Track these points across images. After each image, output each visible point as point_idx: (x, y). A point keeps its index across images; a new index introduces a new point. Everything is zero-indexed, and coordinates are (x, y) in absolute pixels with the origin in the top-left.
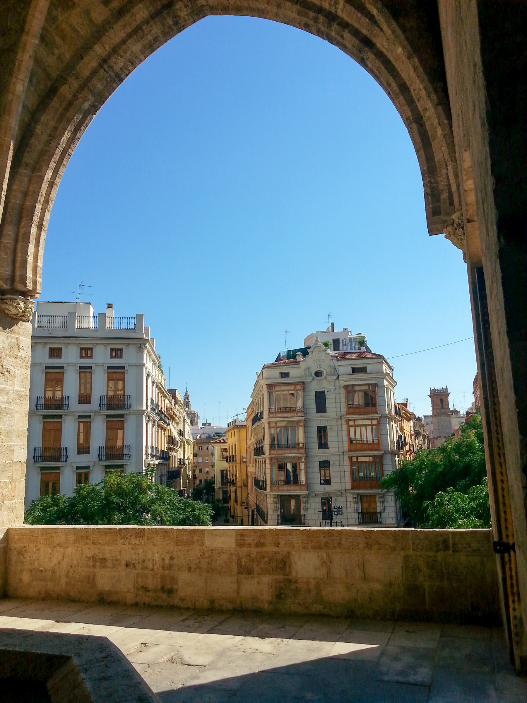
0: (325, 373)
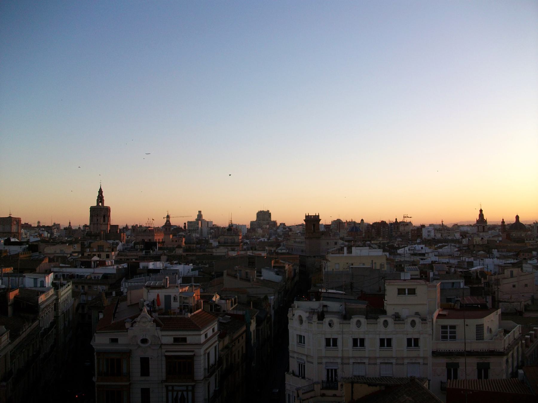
0: (150, 342)
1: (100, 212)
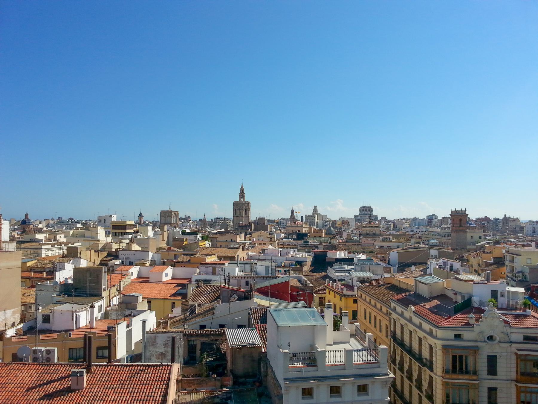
0: (498, 339)
1: (241, 207)
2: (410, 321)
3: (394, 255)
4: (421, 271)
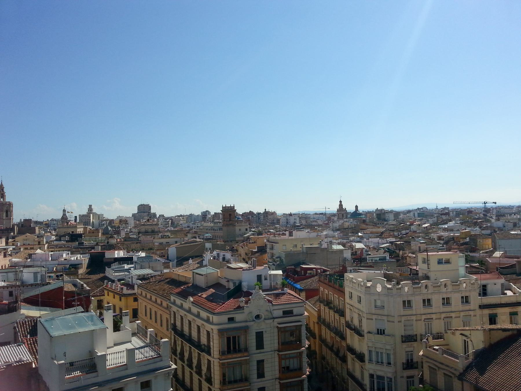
0: (263, 317)
2: (189, 311)
3: (172, 251)
4: (198, 263)
